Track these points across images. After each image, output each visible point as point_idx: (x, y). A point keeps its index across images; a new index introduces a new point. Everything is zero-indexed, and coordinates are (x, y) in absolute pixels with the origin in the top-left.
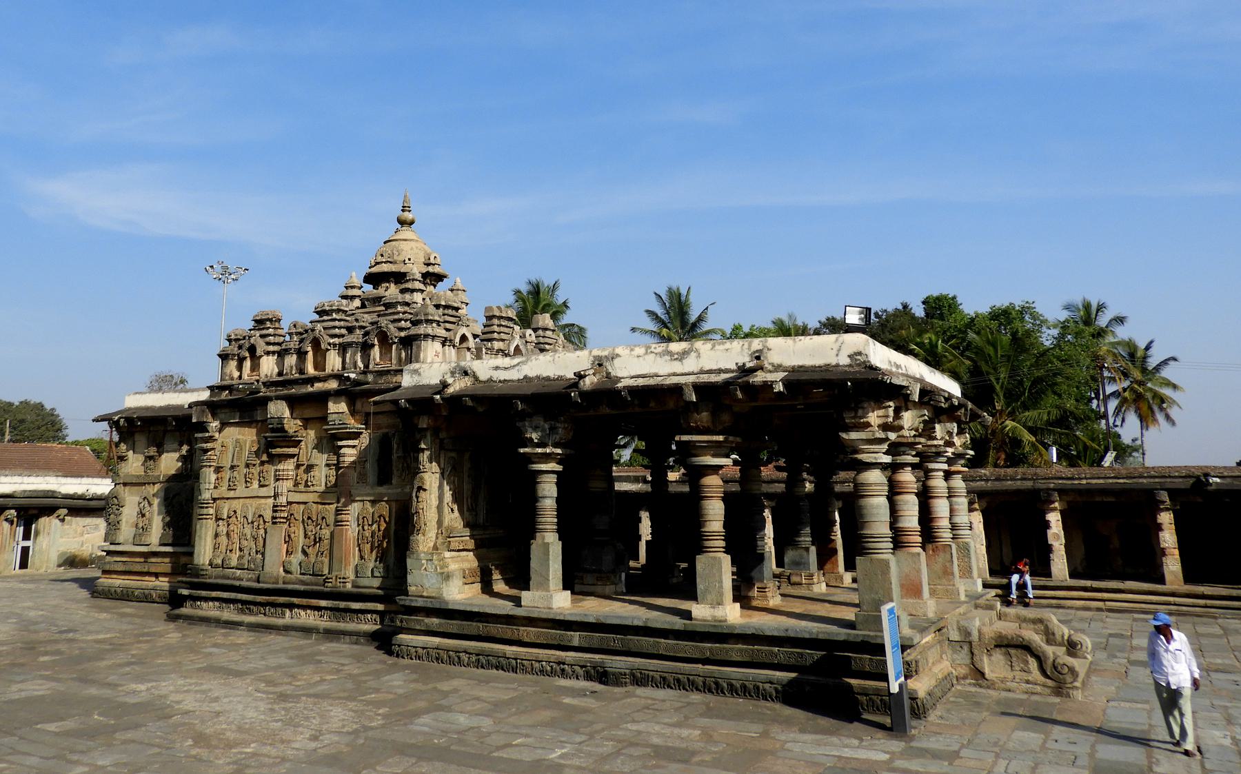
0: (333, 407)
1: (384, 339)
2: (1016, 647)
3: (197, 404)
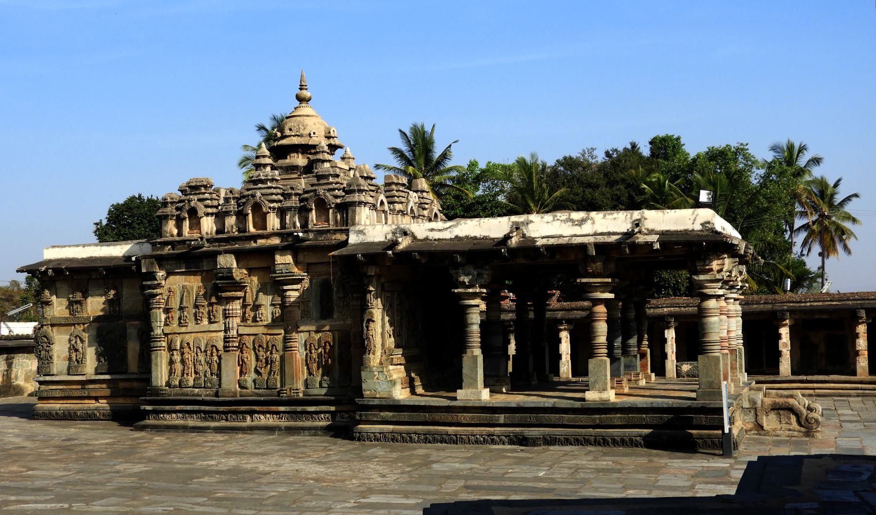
0: (279, 259)
1: (322, 206)
2: (784, 409)
3: (145, 257)
